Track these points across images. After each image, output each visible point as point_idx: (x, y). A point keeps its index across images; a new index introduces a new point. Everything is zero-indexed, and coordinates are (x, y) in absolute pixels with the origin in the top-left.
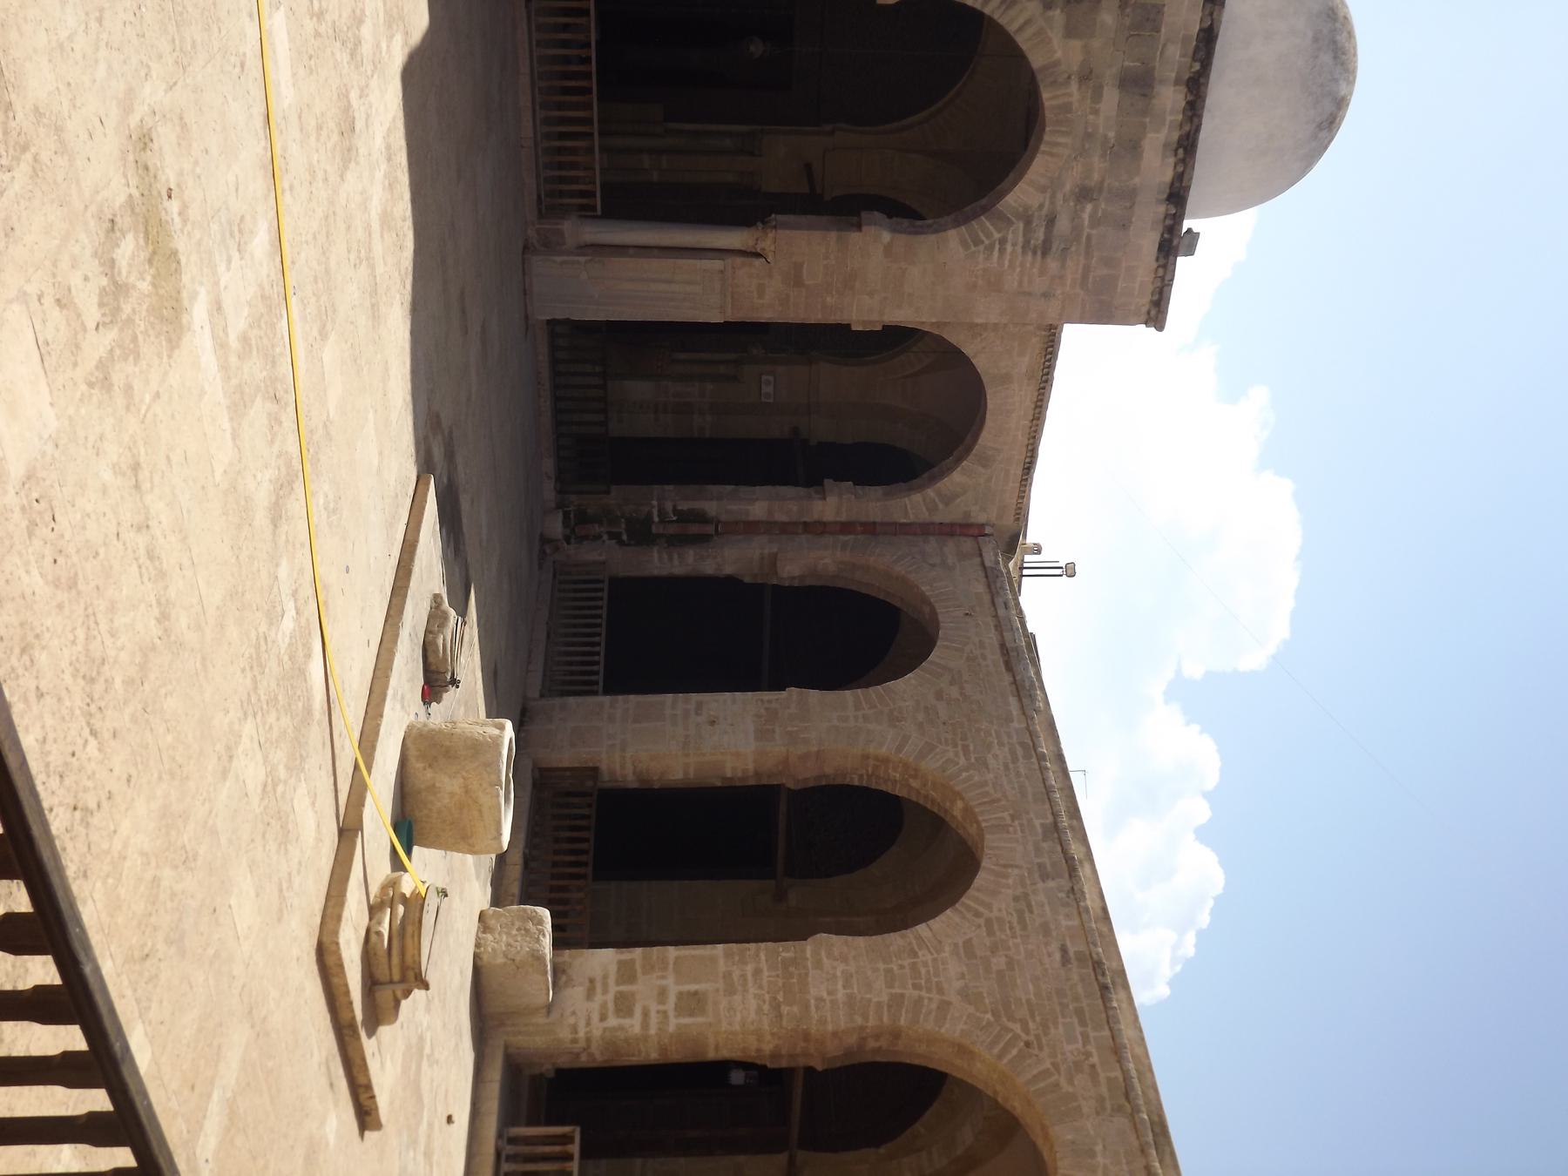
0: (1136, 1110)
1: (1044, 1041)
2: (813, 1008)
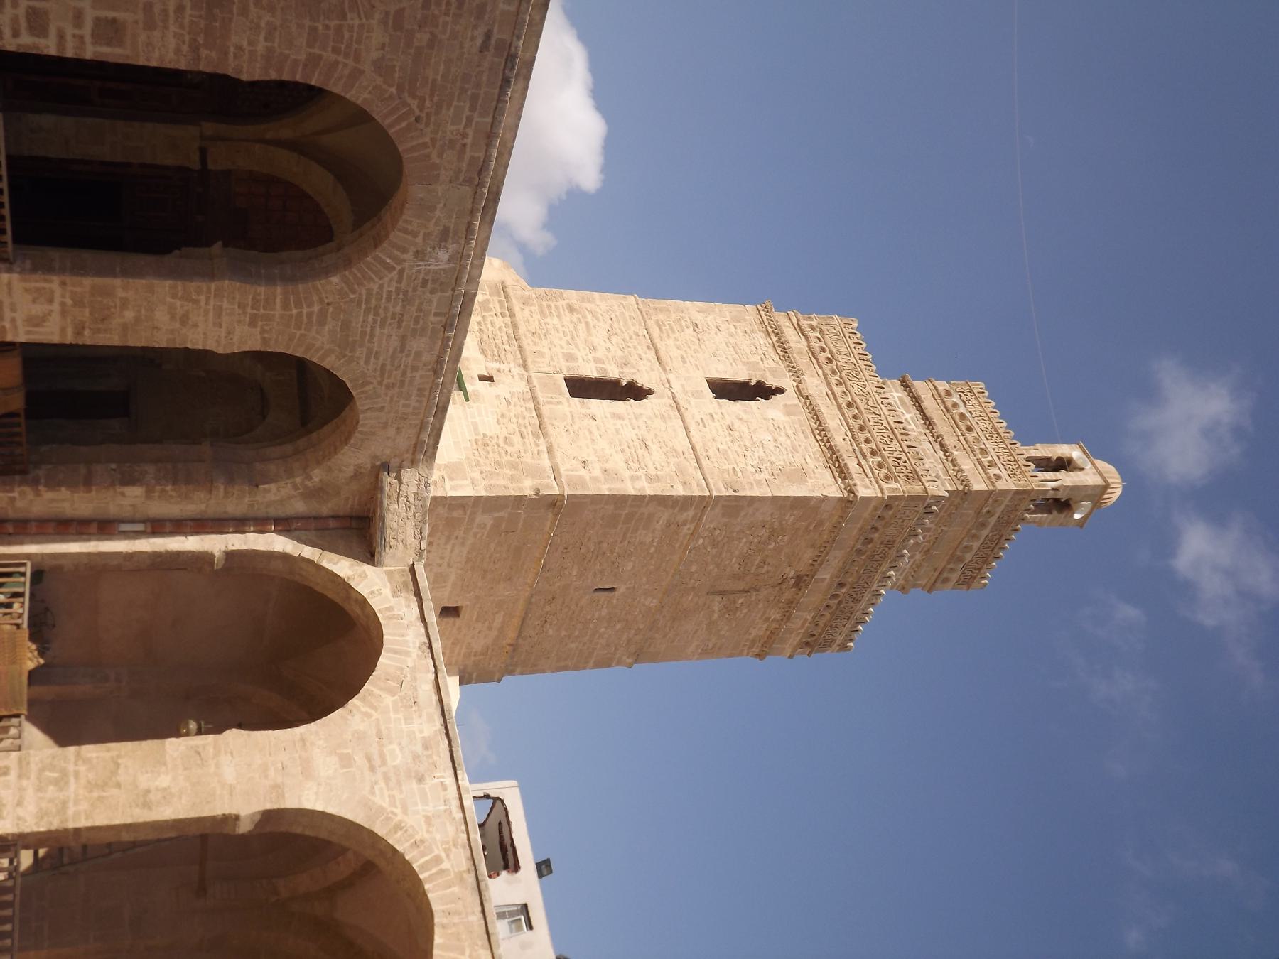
0: (480, 185)
1: (433, 119)
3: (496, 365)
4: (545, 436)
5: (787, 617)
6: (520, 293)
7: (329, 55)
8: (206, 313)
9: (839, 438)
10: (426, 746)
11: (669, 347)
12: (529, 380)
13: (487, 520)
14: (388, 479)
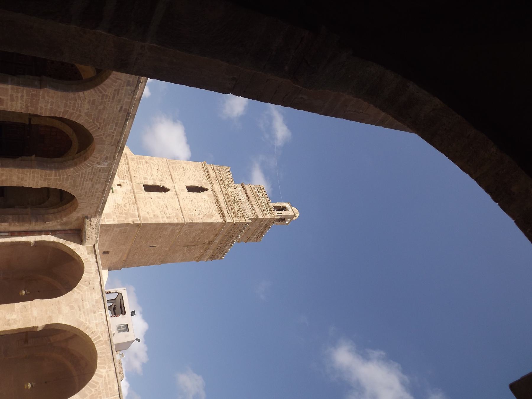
2: (39, 109)
3: (122, 181)
4: (137, 204)
5: (205, 251)
6: (131, 157)
7: (71, 110)
8: (29, 178)
9: (223, 205)
10: (97, 302)
11: (175, 175)
12: (132, 186)
13: (118, 230)
14: (87, 221)
